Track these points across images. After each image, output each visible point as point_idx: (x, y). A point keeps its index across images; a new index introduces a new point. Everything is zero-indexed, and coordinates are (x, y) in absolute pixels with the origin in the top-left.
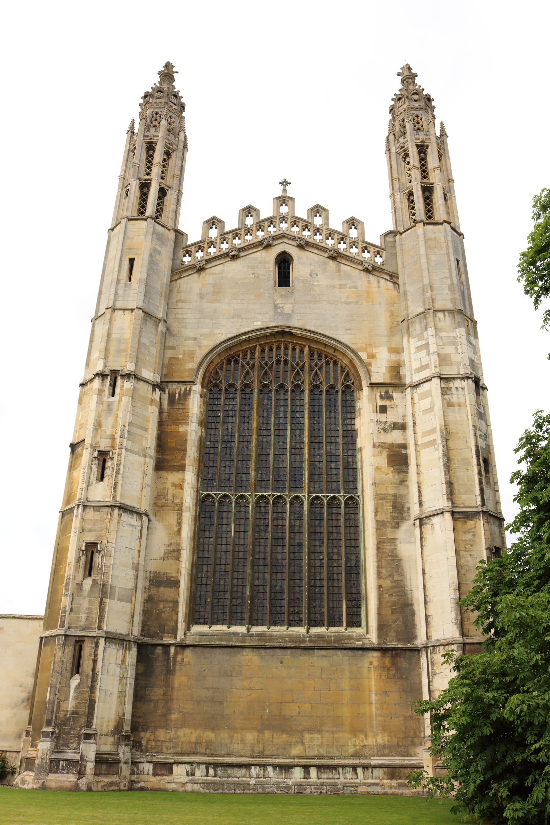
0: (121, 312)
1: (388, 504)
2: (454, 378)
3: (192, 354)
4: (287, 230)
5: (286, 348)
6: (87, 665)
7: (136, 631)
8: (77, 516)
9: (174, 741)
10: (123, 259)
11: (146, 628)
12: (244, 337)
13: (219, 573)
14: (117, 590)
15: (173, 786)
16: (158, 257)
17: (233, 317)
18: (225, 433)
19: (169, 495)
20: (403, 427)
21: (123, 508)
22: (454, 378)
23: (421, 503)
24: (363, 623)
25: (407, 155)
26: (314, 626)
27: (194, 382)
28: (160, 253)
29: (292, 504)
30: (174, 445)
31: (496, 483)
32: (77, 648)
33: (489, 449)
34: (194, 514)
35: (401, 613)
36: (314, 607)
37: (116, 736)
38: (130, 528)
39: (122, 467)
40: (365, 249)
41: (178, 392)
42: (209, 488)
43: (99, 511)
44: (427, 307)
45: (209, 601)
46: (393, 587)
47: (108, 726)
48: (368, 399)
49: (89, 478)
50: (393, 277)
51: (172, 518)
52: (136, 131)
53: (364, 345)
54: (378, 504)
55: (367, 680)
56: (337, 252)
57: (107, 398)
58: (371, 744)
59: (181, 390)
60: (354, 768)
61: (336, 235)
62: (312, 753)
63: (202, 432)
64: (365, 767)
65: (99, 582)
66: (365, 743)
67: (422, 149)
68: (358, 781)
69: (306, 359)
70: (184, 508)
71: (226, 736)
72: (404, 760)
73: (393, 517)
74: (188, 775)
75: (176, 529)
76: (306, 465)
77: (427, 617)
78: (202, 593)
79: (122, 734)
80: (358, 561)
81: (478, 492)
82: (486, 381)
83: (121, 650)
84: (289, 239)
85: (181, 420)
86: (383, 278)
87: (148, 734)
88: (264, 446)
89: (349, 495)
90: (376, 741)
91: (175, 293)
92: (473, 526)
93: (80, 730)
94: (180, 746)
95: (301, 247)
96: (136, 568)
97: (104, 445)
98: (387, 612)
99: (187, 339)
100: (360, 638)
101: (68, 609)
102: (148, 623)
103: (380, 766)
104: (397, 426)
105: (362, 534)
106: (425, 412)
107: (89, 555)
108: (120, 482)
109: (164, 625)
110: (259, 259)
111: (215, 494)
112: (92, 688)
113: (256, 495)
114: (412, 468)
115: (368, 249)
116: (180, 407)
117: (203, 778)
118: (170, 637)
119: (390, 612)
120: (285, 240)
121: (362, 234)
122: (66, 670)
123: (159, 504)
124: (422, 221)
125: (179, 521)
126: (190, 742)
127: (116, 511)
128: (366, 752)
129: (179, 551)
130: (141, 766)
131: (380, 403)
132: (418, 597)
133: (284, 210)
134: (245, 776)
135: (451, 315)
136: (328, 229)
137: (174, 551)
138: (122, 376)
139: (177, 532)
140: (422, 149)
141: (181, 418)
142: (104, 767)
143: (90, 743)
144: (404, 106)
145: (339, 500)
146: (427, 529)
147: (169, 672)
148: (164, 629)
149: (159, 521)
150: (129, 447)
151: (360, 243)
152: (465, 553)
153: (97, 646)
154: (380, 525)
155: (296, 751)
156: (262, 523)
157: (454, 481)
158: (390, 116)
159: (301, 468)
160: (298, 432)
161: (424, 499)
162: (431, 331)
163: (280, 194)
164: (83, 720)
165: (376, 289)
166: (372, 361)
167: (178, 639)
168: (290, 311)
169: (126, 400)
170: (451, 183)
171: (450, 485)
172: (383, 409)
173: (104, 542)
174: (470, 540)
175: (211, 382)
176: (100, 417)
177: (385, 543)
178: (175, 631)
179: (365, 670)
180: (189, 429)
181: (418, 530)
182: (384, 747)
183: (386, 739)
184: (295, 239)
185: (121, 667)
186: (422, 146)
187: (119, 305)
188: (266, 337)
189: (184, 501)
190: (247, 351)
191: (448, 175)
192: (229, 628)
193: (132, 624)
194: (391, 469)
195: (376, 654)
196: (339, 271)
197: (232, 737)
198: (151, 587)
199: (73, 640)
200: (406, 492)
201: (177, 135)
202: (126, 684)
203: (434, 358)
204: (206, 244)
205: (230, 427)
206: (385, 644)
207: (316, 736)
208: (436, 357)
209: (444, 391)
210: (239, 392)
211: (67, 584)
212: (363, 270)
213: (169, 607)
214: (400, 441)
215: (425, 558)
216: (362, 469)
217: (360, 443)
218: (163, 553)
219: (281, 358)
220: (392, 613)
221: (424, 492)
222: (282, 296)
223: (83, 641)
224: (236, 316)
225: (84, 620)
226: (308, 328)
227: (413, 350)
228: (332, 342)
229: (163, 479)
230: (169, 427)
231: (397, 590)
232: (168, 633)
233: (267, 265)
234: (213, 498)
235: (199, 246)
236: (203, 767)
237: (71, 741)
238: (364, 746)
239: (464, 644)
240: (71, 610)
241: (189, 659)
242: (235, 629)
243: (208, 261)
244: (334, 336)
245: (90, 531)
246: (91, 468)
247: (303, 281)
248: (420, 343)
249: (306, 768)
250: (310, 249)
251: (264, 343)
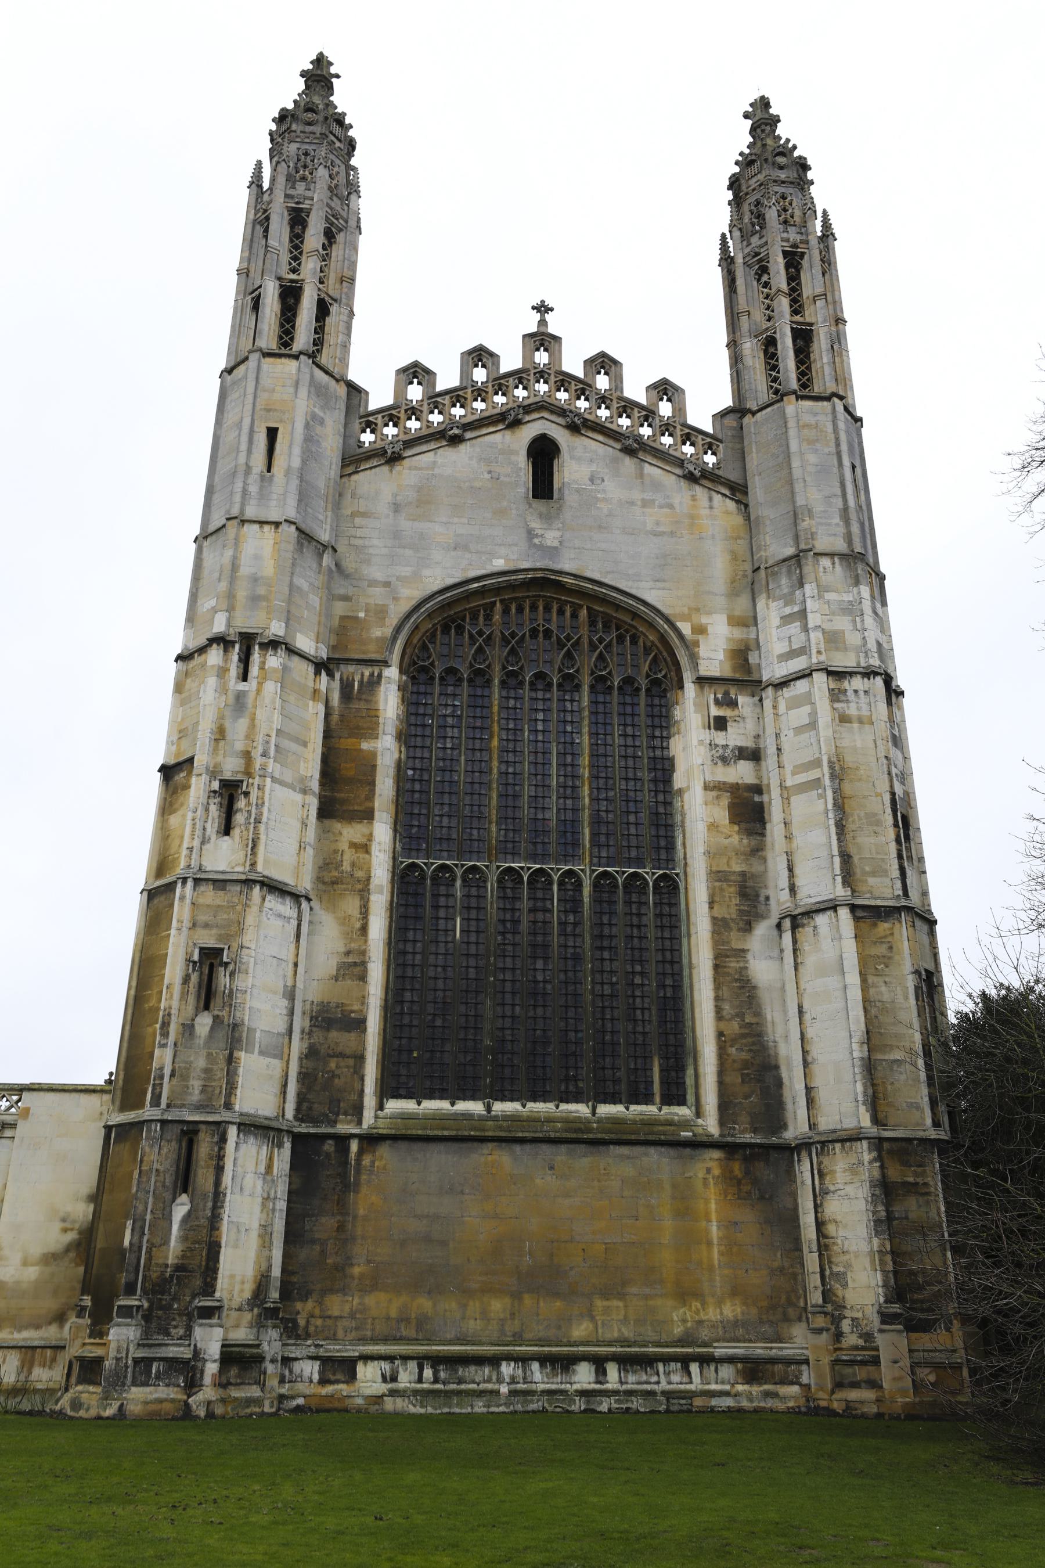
0: (256, 527)
1: (732, 889)
2: (851, 674)
3: (381, 612)
4: (550, 396)
5: (547, 609)
6: (204, 1178)
7: (290, 1114)
8: (182, 898)
9: (358, 1316)
10: (256, 429)
11: (305, 1105)
12: (476, 585)
13: (432, 1005)
14: (258, 1034)
15: (359, 1401)
16: (318, 429)
17: (455, 549)
18: (441, 755)
19: (345, 863)
20: (754, 755)
21: (268, 886)
22: (851, 674)
23: (793, 889)
24: (690, 1098)
25: (764, 270)
26: (605, 1102)
27: (386, 662)
28: (322, 422)
29: (561, 883)
30: (351, 773)
31: (921, 859)
32: (184, 1144)
33: (909, 798)
34: (389, 899)
35: (759, 1081)
36: (603, 1068)
37: (256, 1310)
38: (279, 923)
39: (265, 810)
40: (686, 438)
41: (357, 678)
42: (414, 853)
43: (224, 889)
44: (803, 546)
45: (415, 1055)
46: (743, 1036)
47: (242, 1291)
48: (695, 704)
49: (204, 829)
50: (738, 491)
51: (351, 905)
52: (266, 185)
53: (686, 610)
54: (714, 888)
55: (702, 1201)
56: (638, 439)
57: (235, 685)
58: (713, 1318)
59: (362, 675)
60: (685, 1361)
61: (636, 410)
62: (608, 1336)
63: (400, 752)
64: (705, 1360)
65: (226, 1019)
66: (703, 1316)
67: (793, 260)
68: (692, 1387)
69: (584, 631)
70: (372, 887)
71: (454, 1305)
72: (771, 1348)
73: (741, 912)
74: (384, 1380)
75: (358, 925)
76: (586, 816)
77: (809, 1090)
78: (404, 1041)
79: (267, 1305)
80: (678, 987)
81: (896, 874)
82: (902, 681)
83: (265, 1148)
84: (552, 412)
85: (363, 729)
86: (718, 492)
87: (310, 1304)
88: (511, 781)
89: (662, 872)
90: (721, 1313)
91: (348, 498)
92: (888, 932)
93: (190, 1302)
94: (369, 1326)
95: (574, 428)
96: (290, 995)
97: (231, 768)
98: (734, 1078)
99: (373, 583)
100: (685, 1124)
101: (167, 1072)
102: (309, 1096)
103: (730, 1360)
104: (745, 754)
105: (684, 941)
106: (799, 730)
107: (206, 971)
108: (263, 837)
109: (339, 1101)
110: (500, 446)
111: (425, 864)
112: (215, 1220)
113: (498, 867)
114: (775, 829)
115: (693, 439)
116: (362, 705)
117: (413, 1385)
118: (349, 1122)
119: (740, 1080)
120: (546, 415)
121: (680, 410)
122: (164, 1186)
123: (326, 880)
124: (794, 392)
125: (364, 910)
126: (388, 1318)
127: (257, 889)
128: (704, 1334)
129: (363, 964)
130: (297, 1367)
131: (715, 711)
132: (788, 1053)
133: (542, 358)
134: (489, 1381)
135: (844, 563)
136: (621, 398)
137: (355, 964)
138: (261, 645)
139: (359, 930)
140: (793, 260)
141: (365, 725)
142: (234, 1371)
143: (211, 1326)
144: (760, 177)
145: (645, 879)
146: (805, 933)
147: (346, 1185)
148: (339, 1107)
149: (327, 909)
150: (277, 775)
151: (679, 427)
152: (876, 979)
153: (223, 1139)
154: (719, 925)
155: (580, 1331)
156: (508, 916)
157: (852, 850)
158: (729, 195)
159: (575, 822)
160: (569, 759)
161: (799, 882)
162: (809, 589)
163: (534, 329)
164: (198, 1282)
165: (707, 512)
166: (700, 638)
167: (365, 1126)
168: (556, 544)
169: (271, 687)
170: (840, 326)
171: (846, 858)
172: (720, 724)
173: (235, 946)
174: (884, 957)
175: (415, 663)
176: (222, 717)
177: (728, 957)
178: (358, 1110)
179: (699, 1185)
180: (379, 745)
181: (787, 937)
182: (736, 1323)
183: (739, 1310)
184: (561, 411)
185: (264, 1179)
186: (794, 253)
187: (250, 512)
188: (512, 587)
189: (372, 875)
190: (479, 611)
191: (835, 310)
192: (453, 1104)
193: (284, 1098)
194: (736, 828)
195: (716, 1154)
196: (641, 475)
197: (465, 1306)
198: (314, 1029)
199: (177, 1129)
200: (761, 868)
201: (345, 200)
202: (274, 1210)
203: (816, 637)
204: (403, 411)
205: (449, 745)
206: (732, 1136)
207: (616, 1303)
208: (820, 635)
209: (836, 696)
210: (465, 684)
211: (165, 1025)
212: (684, 477)
213: (348, 1067)
214: (750, 779)
215: (802, 986)
216: (683, 826)
217: (679, 780)
218: (335, 968)
219: (538, 625)
220: (743, 1082)
221: (797, 871)
222: (541, 516)
223: (196, 1132)
224: (460, 546)
225: (197, 1092)
226: (588, 574)
227: (775, 621)
228: (631, 602)
229: (334, 833)
230: (342, 740)
231: (750, 1040)
232: (346, 1114)
233: (513, 458)
234: (422, 869)
235: (391, 415)
236: (413, 1365)
237: (174, 1323)
238: (700, 1322)
239: (881, 1140)
240: (173, 1075)
241: (383, 1162)
242: (462, 1106)
243: (409, 444)
244: (633, 592)
245: (206, 926)
246: (207, 810)
247: (578, 491)
248: (788, 610)
249: (599, 1363)
250: (590, 434)
251: (509, 599)
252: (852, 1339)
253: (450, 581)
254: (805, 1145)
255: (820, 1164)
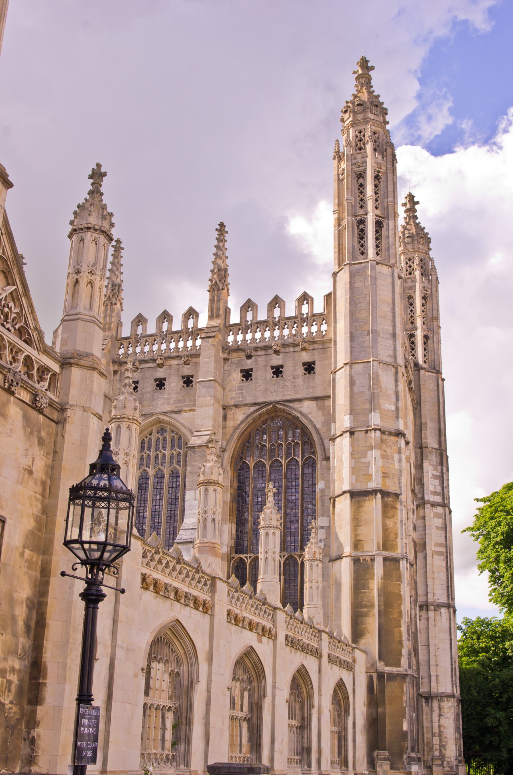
106: (438, 528)
248: (435, 473)
252: (447, 769)
254: (436, 697)
255: (439, 704)
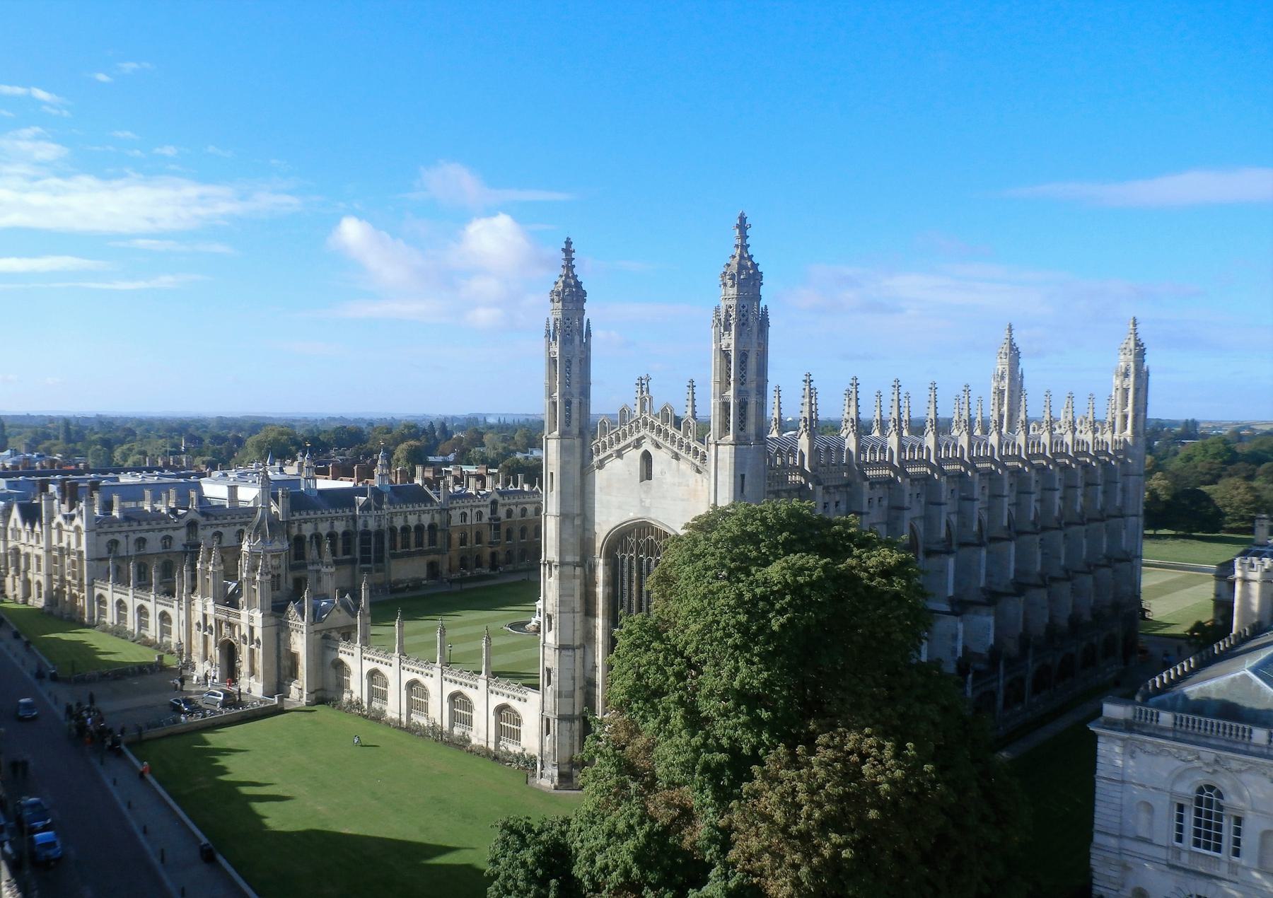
96: (574, 679)
168: (649, 506)
253: (618, 523)
